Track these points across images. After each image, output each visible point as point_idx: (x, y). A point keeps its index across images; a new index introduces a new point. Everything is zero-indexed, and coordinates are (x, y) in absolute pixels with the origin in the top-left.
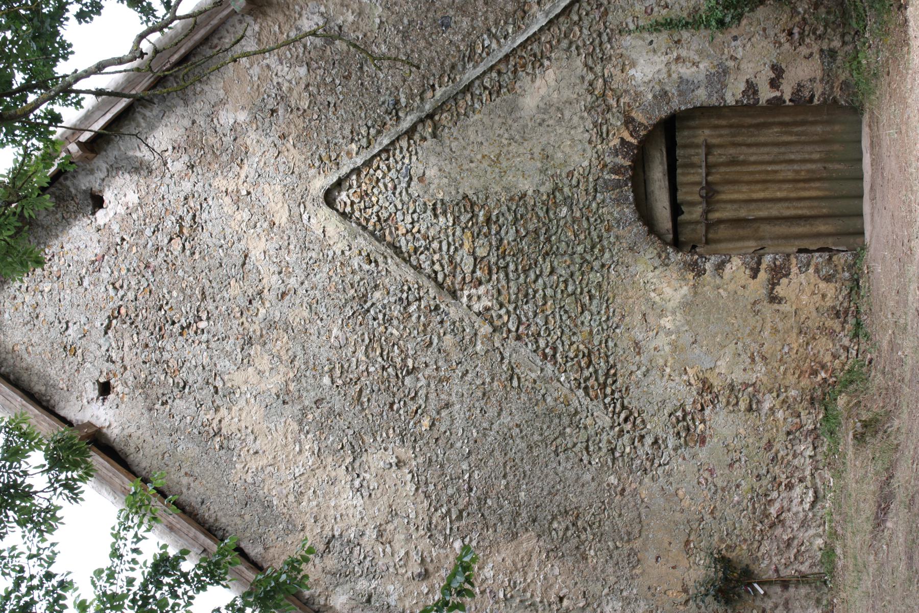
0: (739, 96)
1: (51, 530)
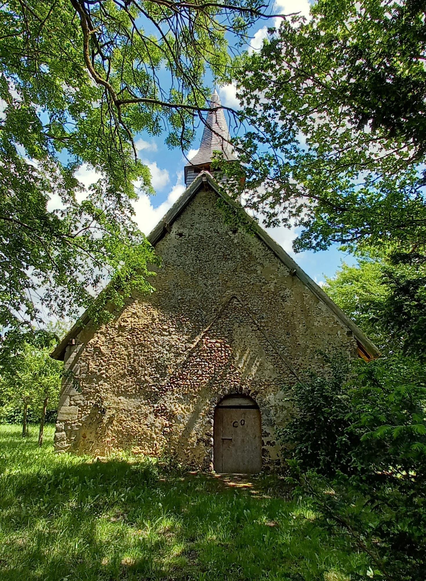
0: (264, 430)
1: (87, 202)
